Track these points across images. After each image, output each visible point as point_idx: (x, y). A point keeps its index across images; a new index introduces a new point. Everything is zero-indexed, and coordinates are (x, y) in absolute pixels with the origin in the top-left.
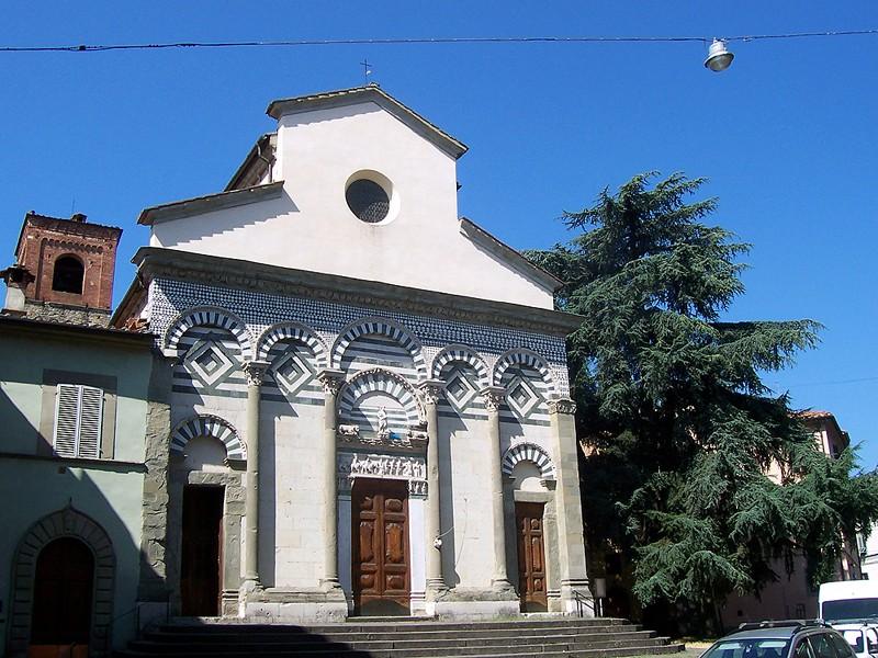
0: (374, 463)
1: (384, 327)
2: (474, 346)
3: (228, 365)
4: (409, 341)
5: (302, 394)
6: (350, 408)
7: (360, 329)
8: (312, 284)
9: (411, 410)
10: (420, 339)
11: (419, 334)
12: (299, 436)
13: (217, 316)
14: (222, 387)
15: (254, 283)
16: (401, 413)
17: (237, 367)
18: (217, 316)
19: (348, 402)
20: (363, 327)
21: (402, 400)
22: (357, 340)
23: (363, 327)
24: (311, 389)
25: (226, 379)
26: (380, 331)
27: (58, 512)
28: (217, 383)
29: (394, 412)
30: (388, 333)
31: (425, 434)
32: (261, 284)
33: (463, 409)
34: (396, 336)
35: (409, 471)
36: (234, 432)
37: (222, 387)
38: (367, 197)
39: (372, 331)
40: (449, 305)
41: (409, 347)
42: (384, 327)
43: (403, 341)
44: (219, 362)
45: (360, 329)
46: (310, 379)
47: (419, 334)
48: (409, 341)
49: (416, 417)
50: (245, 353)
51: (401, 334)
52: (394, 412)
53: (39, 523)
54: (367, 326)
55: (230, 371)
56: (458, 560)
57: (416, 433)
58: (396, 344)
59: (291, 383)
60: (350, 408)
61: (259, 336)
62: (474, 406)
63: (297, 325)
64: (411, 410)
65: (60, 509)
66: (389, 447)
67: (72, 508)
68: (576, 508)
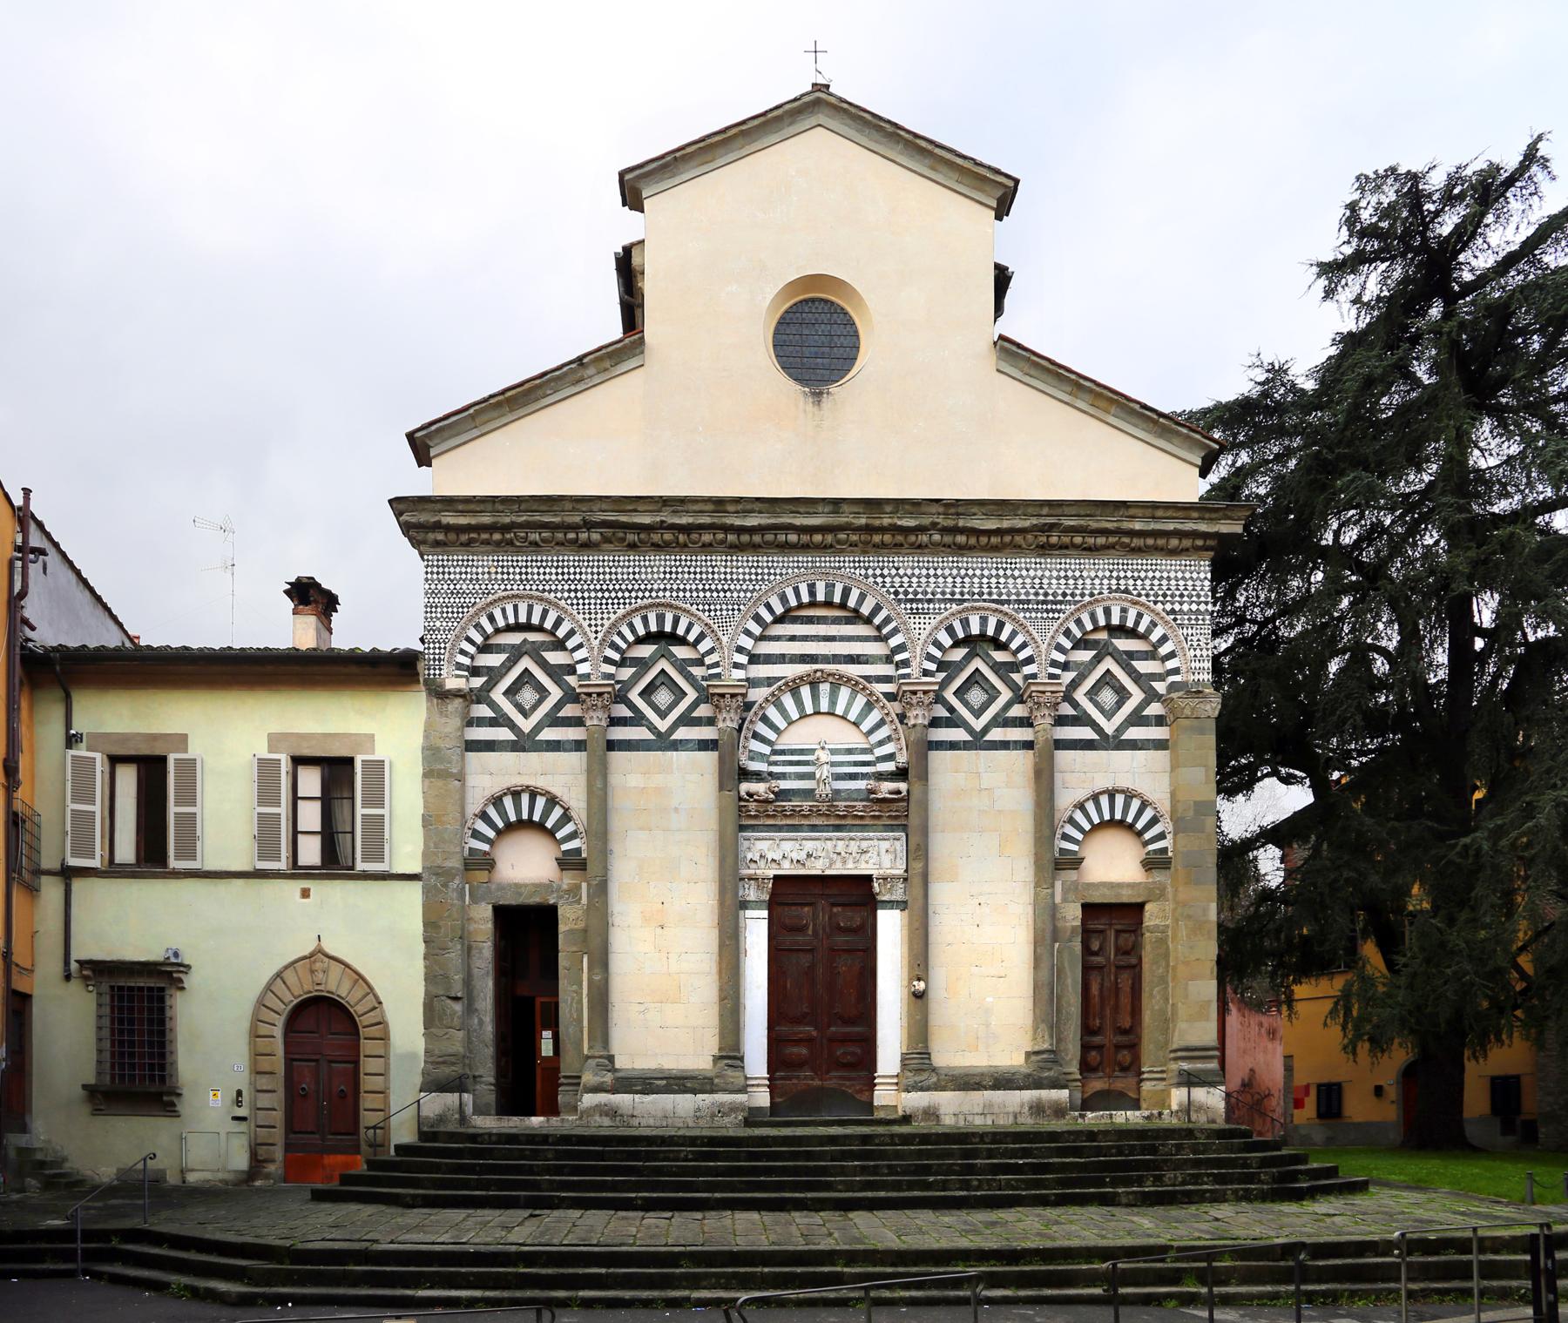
2: (1008, 602)
3: (556, 693)
4: (877, 609)
5: (682, 733)
11: (896, 593)
13: (530, 608)
14: (548, 734)
17: (571, 696)
18: (530, 608)
19: (764, 740)
22: (779, 620)
24: (698, 722)
25: (553, 720)
27: (304, 958)
28: (538, 728)
33: (986, 730)
34: (852, 603)
36: (566, 810)
37: (548, 734)
38: (816, 336)
41: (877, 621)
43: (865, 610)
44: (543, 692)
46: (694, 705)
48: (877, 609)
53: (279, 975)
54: (797, 591)
55: (559, 706)
56: (970, 992)
58: (856, 617)
59: (663, 715)
63: (671, 606)
65: (306, 952)
66: (835, 816)
67: (320, 951)
68: (1205, 911)
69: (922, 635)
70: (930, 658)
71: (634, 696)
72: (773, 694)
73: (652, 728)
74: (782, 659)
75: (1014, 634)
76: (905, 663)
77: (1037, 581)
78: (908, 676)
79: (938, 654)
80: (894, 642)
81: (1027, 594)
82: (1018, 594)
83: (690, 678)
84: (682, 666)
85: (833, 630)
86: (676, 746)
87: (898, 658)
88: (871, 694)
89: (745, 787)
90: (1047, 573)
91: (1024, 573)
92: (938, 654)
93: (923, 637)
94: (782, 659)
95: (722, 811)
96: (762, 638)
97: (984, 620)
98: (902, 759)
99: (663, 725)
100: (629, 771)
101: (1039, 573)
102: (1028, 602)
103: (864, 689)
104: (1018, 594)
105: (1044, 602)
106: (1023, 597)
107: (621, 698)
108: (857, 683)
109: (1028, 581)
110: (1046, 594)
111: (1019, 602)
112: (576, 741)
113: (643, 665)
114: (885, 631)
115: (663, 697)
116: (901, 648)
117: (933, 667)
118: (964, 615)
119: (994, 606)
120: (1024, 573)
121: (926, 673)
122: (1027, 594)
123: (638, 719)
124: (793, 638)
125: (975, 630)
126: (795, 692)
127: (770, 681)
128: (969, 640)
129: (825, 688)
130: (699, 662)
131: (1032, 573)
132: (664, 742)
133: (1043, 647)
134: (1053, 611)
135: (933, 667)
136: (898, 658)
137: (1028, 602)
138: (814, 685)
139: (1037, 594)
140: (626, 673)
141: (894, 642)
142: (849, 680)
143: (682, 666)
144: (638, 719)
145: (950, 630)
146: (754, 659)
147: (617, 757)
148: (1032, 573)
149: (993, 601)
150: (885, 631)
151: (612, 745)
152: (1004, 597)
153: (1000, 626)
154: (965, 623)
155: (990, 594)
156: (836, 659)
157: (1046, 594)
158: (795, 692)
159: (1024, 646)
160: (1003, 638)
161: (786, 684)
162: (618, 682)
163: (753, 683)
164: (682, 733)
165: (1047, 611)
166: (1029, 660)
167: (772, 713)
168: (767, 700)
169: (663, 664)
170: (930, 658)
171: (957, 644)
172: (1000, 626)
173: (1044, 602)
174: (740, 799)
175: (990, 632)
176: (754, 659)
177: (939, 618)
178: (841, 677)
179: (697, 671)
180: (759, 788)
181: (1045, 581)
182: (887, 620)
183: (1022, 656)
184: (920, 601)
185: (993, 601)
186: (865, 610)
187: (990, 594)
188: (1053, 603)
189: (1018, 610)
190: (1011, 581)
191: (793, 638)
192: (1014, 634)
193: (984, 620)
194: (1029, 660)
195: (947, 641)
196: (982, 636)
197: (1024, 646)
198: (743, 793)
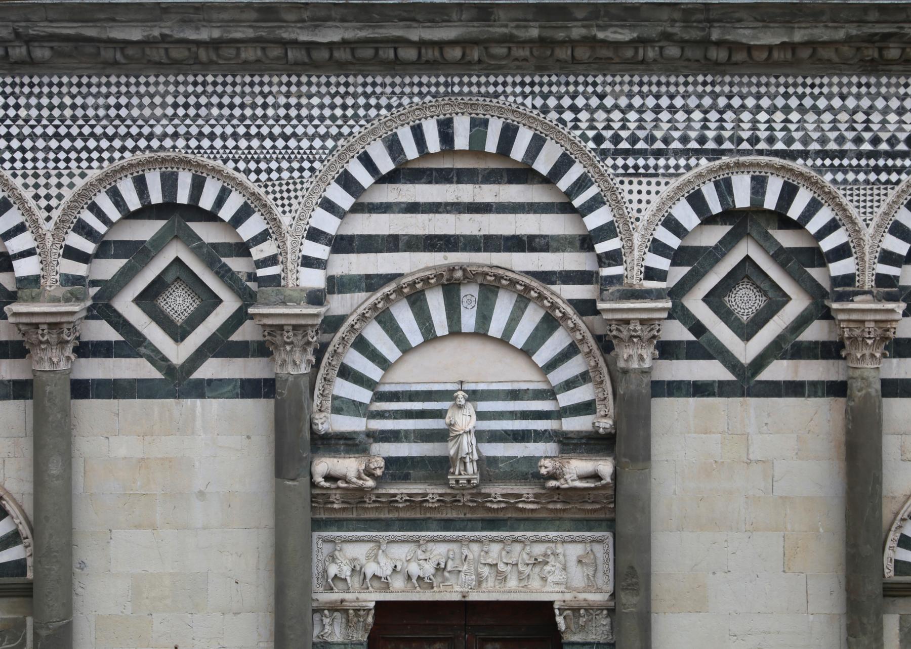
0: (439, 551)
1: (479, 127)
2: (805, 155)
4: (563, 164)
5: (210, 369)
6: (363, 395)
7: (394, 147)
8: (204, 35)
9: (569, 385)
10: (604, 154)
12: (201, 494)
15: (18, 52)
16: (550, 394)
20: (406, 137)
21: (543, 356)
23: (406, 137)
26: (461, 142)
29: (514, 395)
30: (491, 145)
31: (605, 467)
32: (41, 53)
34: (518, 152)
35: (559, 572)
39: (433, 144)
40: (695, 34)
41: (564, 184)
42: (479, 127)
43: (543, 165)
45: (394, 147)
47: (599, 139)
48: (563, 164)
49: (586, 408)
50: (25, 268)
51: (537, 144)
52: (514, 395)
57: (577, 467)
58: (523, 174)
59: (178, 333)
60: (363, 395)
61: (55, 214)
62: (801, 352)
64: (569, 385)
69: (648, 209)
70: (658, 248)
71: (126, 304)
72: (374, 307)
73: (157, 358)
74: (392, 243)
75: (813, 208)
76: (614, 258)
77: (860, 117)
78: (618, 279)
79: (674, 242)
80: (594, 220)
81: (841, 140)
82: (823, 141)
83: (225, 274)
84: (212, 256)
85: (487, 193)
86: (202, 389)
87: (602, 247)
88: (554, 306)
89: (323, 465)
90: (880, 103)
91: (837, 103)
92: (674, 242)
93: (645, 216)
94: (392, 243)
95: (280, 511)
96: (358, 208)
97: (759, 186)
98: (605, 424)
99: (177, 353)
100: (113, 440)
101: (865, 103)
102: (842, 154)
103: (541, 297)
104: (823, 141)
105: (869, 155)
106: (832, 146)
107: (102, 309)
108: (528, 288)
109: (843, 117)
110: (876, 141)
111: (824, 154)
112: (16, 383)
113: (138, 254)
114: (577, 202)
115: (178, 303)
116: (607, 231)
117: (662, 263)
118: (722, 176)
119: (777, 161)
120: (837, 103)
121: (651, 273)
122: (841, 140)
123: (133, 344)
124: (413, 208)
125: (742, 199)
126: (417, 301)
127: (371, 282)
128: (729, 214)
129: (470, 294)
130: (243, 249)
131: (851, 103)
132: (178, 383)
133: (868, 233)
134: (888, 170)
135: (662, 263)
136: (602, 247)
137: (842, 154)
138: (451, 290)
139: (858, 140)
140: (109, 268)
141: (594, 220)
142: (513, 283)
143: (212, 256)
144: (133, 344)
145: (697, 201)
146: (342, 244)
147: (91, 410)
148: (851, 103)
149: (777, 153)
150: (577, 202)
151: (82, 389)
152: (797, 146)
153: (788, 194)
154: (725, 189)
155: (771, 140)
156: (491, 243)
157: (876, 141)
158: (417, 301)
159: (831, 227)
160: (794, 212)
161: (399, 290)
162: (94, 283)
163: (336, 285)
164: (210, 369)
165: (877, 170)
166: (842, 252)
167: (375, 335)
168: (363, 318)
169: (175, 251)
170: (658, 248)
171: (708, 220)
172: (788, 194)
173: (869, 155)
174: (313, 485)
175: (770, 202)
176: (342, 244)
177: (675, 183)
178: (498, 278)
179: (236, 264)
180: (348, 466)
181: (876, 117)
182: (582, 184)
183: (827, 245)
184: (643, 153)
185: (777, 153)
186: (543, 165)
187: (771, 140)
188: (888, 155)
189: (821, 170)
190: (811, 117)
191: (413, 208)
192: (813, 208)
193: (759, 186)
194: (842, 252)
195: (687, 217)
196: (756, 210)
197: (831, 227)
198: (319, 479)
